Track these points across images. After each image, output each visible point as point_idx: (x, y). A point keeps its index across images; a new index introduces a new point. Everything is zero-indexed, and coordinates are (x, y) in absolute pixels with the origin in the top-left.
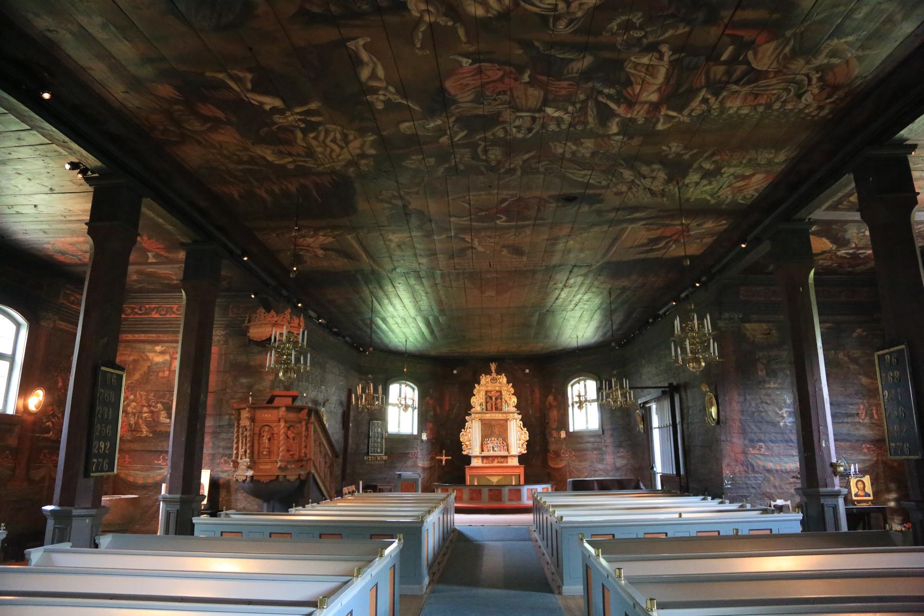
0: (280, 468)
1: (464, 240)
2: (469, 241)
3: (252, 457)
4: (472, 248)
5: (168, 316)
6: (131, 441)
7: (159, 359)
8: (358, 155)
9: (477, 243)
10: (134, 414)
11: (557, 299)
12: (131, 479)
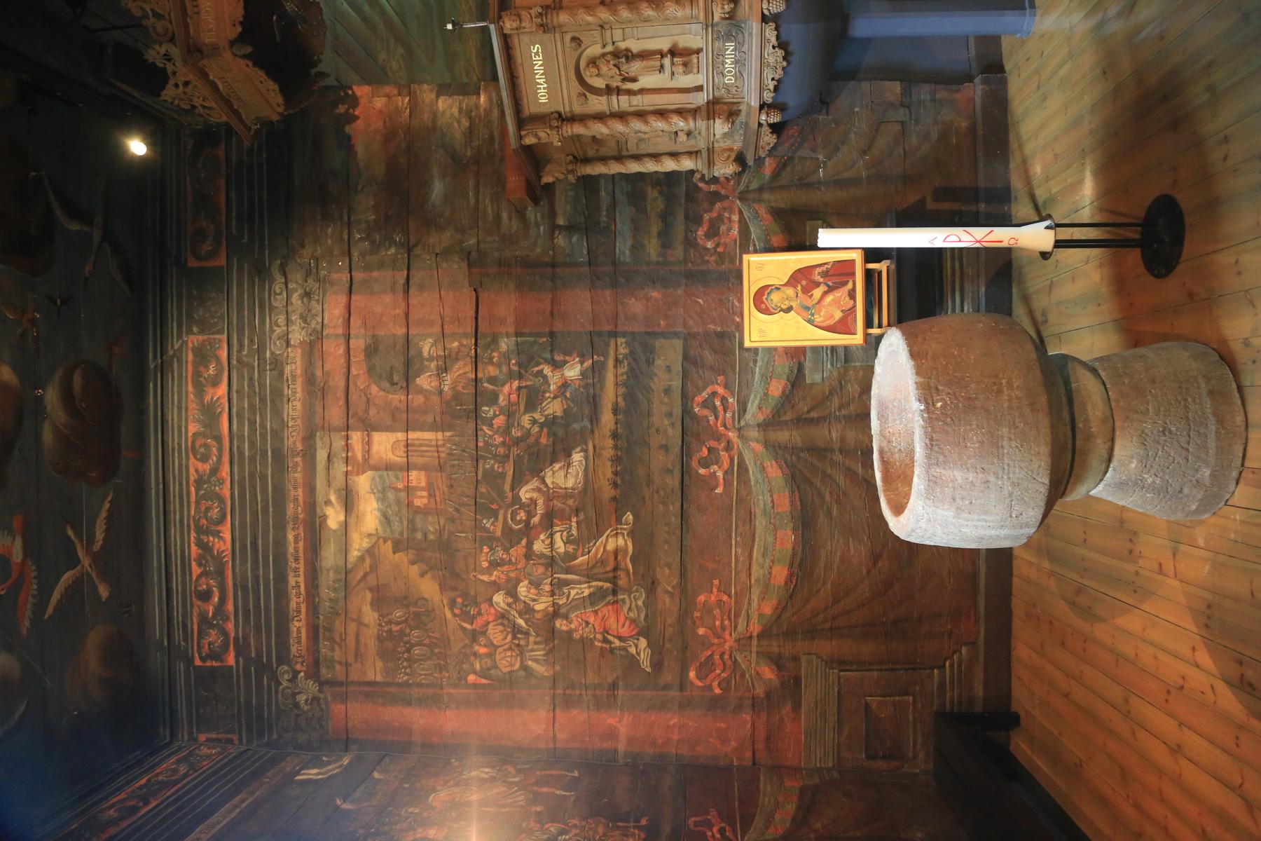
5: (227, 493)
6: (652, 588)
7: (370, 514)
12: (780, 573)
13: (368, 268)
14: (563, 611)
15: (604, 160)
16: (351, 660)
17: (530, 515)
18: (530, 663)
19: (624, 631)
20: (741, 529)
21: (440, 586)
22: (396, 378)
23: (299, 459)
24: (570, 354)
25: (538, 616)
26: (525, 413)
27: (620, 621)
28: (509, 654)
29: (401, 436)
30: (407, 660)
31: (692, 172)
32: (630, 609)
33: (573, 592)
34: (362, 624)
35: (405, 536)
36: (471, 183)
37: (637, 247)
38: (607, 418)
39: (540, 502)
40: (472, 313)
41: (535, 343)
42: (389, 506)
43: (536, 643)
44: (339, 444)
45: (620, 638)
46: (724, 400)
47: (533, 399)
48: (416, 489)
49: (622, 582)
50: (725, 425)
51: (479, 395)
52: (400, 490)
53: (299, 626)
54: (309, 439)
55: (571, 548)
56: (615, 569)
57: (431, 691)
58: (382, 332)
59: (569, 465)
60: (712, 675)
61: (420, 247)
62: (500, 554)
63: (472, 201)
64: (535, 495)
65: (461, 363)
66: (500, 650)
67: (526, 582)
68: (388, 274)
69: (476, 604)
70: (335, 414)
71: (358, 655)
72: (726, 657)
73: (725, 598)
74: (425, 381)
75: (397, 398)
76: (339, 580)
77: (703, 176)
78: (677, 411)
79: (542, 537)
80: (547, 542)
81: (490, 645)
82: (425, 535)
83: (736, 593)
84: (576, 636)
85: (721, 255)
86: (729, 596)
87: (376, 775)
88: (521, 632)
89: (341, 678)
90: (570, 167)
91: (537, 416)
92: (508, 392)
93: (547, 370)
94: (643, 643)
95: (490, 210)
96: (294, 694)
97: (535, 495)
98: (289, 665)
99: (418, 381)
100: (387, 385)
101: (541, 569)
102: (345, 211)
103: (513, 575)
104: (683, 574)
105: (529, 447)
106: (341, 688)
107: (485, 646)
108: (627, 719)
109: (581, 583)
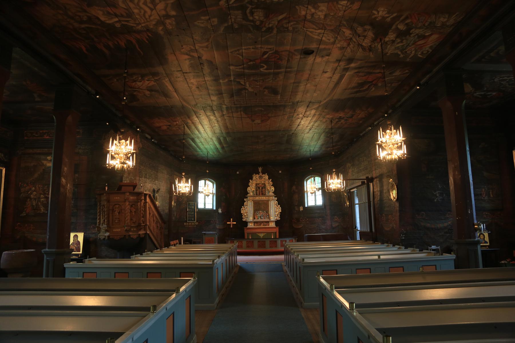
0: (126, 230)
1: (239, 83)
2: (243, 84)
3: (108, 225)
4: (245, 89)
8: (164, 16)
9: (248, 85)
10: (35, 199)
11: (298, 125)
53: (31, 151)
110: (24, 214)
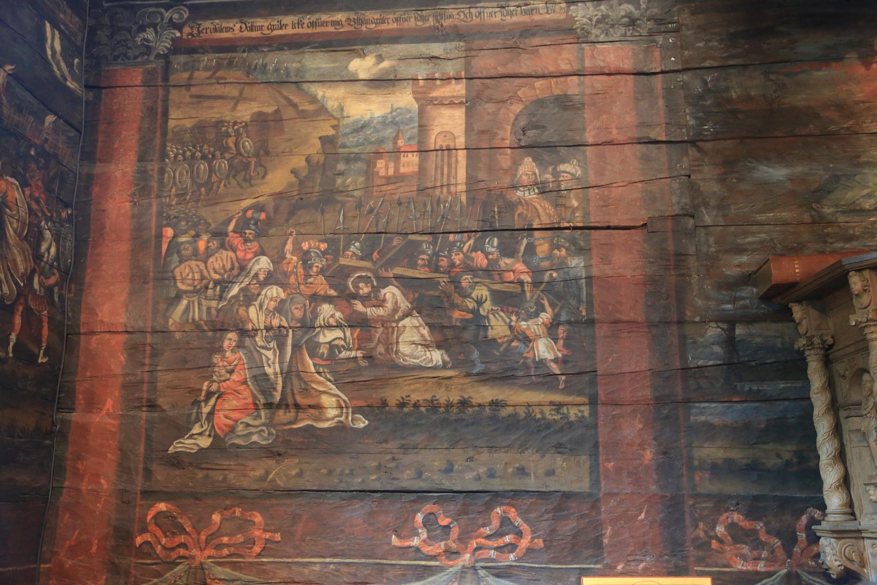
6: (272, 453)
10: (278, 335)
13: (668, 94)
14: (248, 342)
15: (830, 385)
16: (194, 90)
17: (365, 299)
18: (185, 302)
19: (221, 419)
20: (344, 569)
21: (281, 193)
22: (531, 133)
23: (431, 22)
24: (567, 345)
25: (242, 311)
26: (490, 290)
27: (233, 412)
28: (197, 276)
29: (461, 141)
30: (193, 155)
31: (823, 507)
32: (248, 425)
33: (269, 354)
34: (236, 104)
35: (340, 150)
36: (785, 215)
37: (709, 431)
38: (485, 394)
39: (381, 312)
40: (614, 222)
41: (580, 301)
42: (377, 131)
43: (209, 309)
44: (450, 69)
45: (211, 414)
46: (512, 547)
47: (508, 300)
48: (397, 161)
49: (282, 416)
50: (479, 548)
51: (511, 233)
52: (395, 143)
53: (234, 29)
54: (457, 34)
55: (324, 350)
56: (297, 406)
57: (154, 184)
58: (587, 114)
59: (427, 346)
60: (159, 533)
61: (697, 155)
62: (318, 264)
63: (762, 217)
64: (389, 305)
65: (551, 211)
66: (202, 265)
67: (283, 295)
68: (661, 117)
69: (259, 235)
70: (486, 63)
71: (201, 98)
72: (182, 552)
73: (257, 549)
74: (528, 168)
75: (506, 136)
76: (288, 75)
77: (819, 523)
78: (496, 485)
79: (338, 315)
80: (332, 322)
81: (208, 254)
82: (341, 174)
83: (263, 564)
84: (216, 359)
85: (707, 544)
86: (259, 555)
87: (50, 119)
88: (223, 291)
89: (174, 78)
90: (816, 341)
91: (488, 305)
92: (517, 268)
93: (546, 317)
94: (205, 442)
95: (750, 239)
96: (154, 26)
97: (389, 305)
98: (188, 19)
99: (528, 160)
100: (523, 123)
101: (298, 314)
102: (740, 61)
103: (292, 280)
104: (289, 493)
105: (449, 296)
106: (161, 80)
107: (207, 248)
108: (112, 423)
109: (281, 363)
110: (197, 440)
